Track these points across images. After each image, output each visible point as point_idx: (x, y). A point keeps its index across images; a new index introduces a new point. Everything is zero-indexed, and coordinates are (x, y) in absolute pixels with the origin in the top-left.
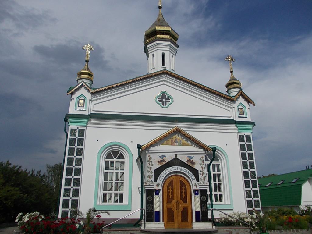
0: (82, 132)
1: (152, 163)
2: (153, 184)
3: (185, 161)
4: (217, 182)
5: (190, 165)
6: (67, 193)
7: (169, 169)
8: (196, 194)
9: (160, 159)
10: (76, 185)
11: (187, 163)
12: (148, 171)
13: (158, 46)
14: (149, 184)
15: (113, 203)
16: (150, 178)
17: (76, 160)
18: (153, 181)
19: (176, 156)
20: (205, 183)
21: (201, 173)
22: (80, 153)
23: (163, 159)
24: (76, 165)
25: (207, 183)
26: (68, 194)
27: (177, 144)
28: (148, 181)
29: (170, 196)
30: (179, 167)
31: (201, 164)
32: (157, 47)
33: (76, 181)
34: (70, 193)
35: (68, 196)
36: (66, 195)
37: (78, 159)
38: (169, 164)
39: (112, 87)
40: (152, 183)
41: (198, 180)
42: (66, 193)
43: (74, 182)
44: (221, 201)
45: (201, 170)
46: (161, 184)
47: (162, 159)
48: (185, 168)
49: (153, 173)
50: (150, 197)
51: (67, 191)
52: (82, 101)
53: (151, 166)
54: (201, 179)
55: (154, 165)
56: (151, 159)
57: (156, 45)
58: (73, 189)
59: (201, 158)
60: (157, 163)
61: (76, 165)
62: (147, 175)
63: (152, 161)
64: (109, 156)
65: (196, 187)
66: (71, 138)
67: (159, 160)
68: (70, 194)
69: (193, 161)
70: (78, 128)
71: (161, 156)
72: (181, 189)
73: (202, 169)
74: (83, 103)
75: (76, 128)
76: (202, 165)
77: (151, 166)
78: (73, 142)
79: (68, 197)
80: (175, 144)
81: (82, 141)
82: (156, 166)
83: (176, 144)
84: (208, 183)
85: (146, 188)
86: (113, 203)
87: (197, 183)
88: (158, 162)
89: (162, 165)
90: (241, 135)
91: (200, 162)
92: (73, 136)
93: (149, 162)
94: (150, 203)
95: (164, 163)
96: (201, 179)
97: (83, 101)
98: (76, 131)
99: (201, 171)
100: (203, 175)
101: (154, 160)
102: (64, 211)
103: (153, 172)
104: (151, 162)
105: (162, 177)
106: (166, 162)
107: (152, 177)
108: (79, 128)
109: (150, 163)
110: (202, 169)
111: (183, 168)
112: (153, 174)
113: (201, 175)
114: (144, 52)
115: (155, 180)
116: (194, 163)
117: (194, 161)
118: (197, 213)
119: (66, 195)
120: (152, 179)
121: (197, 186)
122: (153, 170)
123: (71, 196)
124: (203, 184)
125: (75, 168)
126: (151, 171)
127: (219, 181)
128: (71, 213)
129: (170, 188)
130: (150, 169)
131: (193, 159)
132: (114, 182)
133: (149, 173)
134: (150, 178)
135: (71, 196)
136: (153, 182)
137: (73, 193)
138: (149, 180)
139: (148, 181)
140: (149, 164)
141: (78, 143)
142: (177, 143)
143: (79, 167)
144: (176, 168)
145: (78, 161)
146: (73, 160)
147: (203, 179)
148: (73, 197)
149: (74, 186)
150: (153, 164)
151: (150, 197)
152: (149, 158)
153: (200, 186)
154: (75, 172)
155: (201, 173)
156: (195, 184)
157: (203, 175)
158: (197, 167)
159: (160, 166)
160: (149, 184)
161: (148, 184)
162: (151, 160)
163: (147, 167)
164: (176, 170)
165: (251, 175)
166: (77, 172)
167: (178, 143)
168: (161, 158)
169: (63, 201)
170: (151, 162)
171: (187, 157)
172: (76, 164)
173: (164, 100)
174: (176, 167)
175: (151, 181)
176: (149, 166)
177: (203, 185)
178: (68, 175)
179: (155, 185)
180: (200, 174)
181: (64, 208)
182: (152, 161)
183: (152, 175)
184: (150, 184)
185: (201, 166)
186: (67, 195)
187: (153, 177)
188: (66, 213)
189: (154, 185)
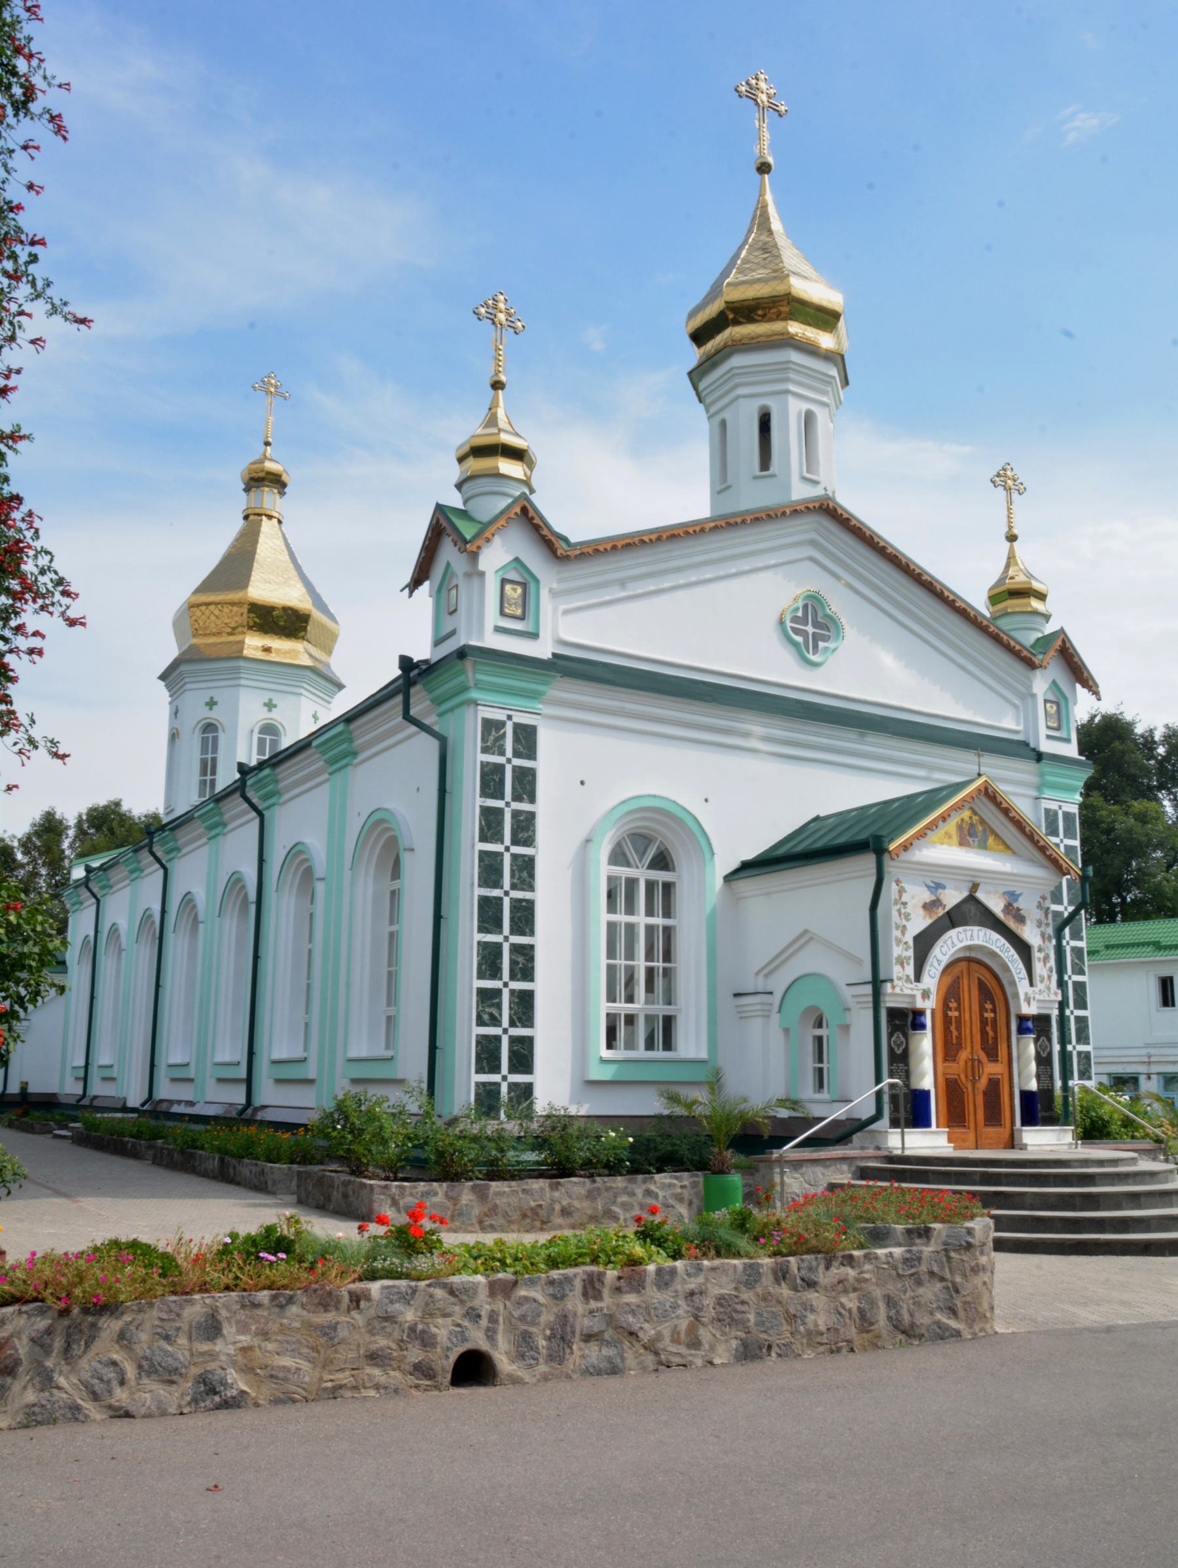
0: (526, 739)
1: (908, 910)
2: (912, 989)
3: (996, 906)
4: (659, 964)
5: (1011, 924)
6: (490, 1006)
7: (953, 933)
8: (1022, 1030)
9: (927, 897)
10: (519, 976)
11: (1001, 916)
12: (899, 942)
13: (792, 375)
14: (902, 990)
15: (641, 1053)
16: (903, 967)
17: (511, 865)
18: (912, 977)
20: (1052, 991)
21: (1041, 955)
22: (526, 835)
24: (514, 887)
25: (1056, 994)
26: (495, 1012)
27: (976, 843)
28: (899, 979)
29: (955, 1033)
31: (1039, 924)
32: (787, 380)
33: (521, 959)
34: (499, 1006)
35: (495, 1021)
36: (486, 1017)
37: (520, 861)
38: (954, 918)
39: (530, 515)
40: (910, 986)
41: (1031, 984)
42: (487, 1010)
43: (511, 960)
44: (668, 1045)
45: (1042, 943)
46: (933, 989)
47: (934, 898)
50: (898, 1037)
51: (488, 997)
52: (515, 590)
53: (904, 922)
54: (1040, 976)
55: (913, 916)
56: (904, 894)
57: (786, 366)
58: (512, 992)
59: (1041, 900)
60: (921, 912)
61: (514, 887)
62: (895, 955)
63: (906, 903)
64: (618, 857)
65: (1029, 1004)
66: (488, 763)
67: (928, 901)
68: (501, 1015)
69: (1018, 909)
70: (510, 717)
71: (933, 885)
72: (982, 1009)
74: (520, 601)
75: (504, 718)
76: (1042, 929)
77: (904, 922)
78: (494, 780)
79: (495, 1026)
80: (970, 840)
81: (531, 778)
82: (919, 922)
84: (1059, 992)
86: (641, 1053)
87: (1030, 990)
88: (926, 907)
89: (935, 918)
90: (1050, 810)
91: (1038, 917)
92: (493, 754)
93: (898, 907)
94: (901, 1060)
95: (941, 912)
96: (1040, 976)
97: (519, 590)
98: (505, 733)
99: (1040, 950)
100: (1045, 965)
101: (913, 897)
102: (484, 1084)
103: (911, 943)
104: (905, 904)
105: (935, 964)
106: (947, 909)
107: (908, 964)
108: (515, 720)
109: (903, 911)
111: (995, 936)
112: (910, 953)
113: (1042, 963)
114: (690, 374)
115: (918, 977)
116: (1021, 919)
117: (1021, 912)
118: (1027, 1096)
119: (486, 1017)
120: (910, 970)
121: (1032, 1000)
122: (909, 938)
123: (505, 1022)
124: (1046, 994)
125: (501, 899)
126: (904, 940)
127: (667, 957)
128: (512, 1094)
129: (953, 1005)
130: (903, 933)
131: (1021, 904)
133: (901, 947)
134: (903, 967)
135: (505, 1022)
137: (511, 1008)
138: (900, 975)
139: (899, 979)
140: (900, 915)
141: (513, 788)
143: (527, 895)
144: (975, 934)
145: (521, 871)
146: (502, 860)
147: (1046, 977)
148: (512, 1024)
149: (513, 977)
150: (909, 914)
151: (898, 1037)
152: (899, 891)
153: (1039, 1001)
154: (512, 919)
155: (1041, 955)
156: (1026, 994)
157: (1045, 965)
158: (1030, 934)
159: (928, 922)
160: (902, 990)
161: (897, 990)
163: (893, 925)
164: (976, 942)
165: (1072, 961)
166: (520, 918)
167: (977, 837)
168: (932, 893)
169: (478, 1043)
170: (905, 904)
171: (1004, 893)
172: (515, 881)
173: (810, 629)
174: (976, 928)
175: (908, 976)
177: (1047, 998)
178: (488, 931)
180: (1039, 959)
181: (484, 1073)
182: (906, 903)
183: (910, 957)
186: (492, 1016)
187: (912, 962)
188: (491, 1091)
189: (915, 992)
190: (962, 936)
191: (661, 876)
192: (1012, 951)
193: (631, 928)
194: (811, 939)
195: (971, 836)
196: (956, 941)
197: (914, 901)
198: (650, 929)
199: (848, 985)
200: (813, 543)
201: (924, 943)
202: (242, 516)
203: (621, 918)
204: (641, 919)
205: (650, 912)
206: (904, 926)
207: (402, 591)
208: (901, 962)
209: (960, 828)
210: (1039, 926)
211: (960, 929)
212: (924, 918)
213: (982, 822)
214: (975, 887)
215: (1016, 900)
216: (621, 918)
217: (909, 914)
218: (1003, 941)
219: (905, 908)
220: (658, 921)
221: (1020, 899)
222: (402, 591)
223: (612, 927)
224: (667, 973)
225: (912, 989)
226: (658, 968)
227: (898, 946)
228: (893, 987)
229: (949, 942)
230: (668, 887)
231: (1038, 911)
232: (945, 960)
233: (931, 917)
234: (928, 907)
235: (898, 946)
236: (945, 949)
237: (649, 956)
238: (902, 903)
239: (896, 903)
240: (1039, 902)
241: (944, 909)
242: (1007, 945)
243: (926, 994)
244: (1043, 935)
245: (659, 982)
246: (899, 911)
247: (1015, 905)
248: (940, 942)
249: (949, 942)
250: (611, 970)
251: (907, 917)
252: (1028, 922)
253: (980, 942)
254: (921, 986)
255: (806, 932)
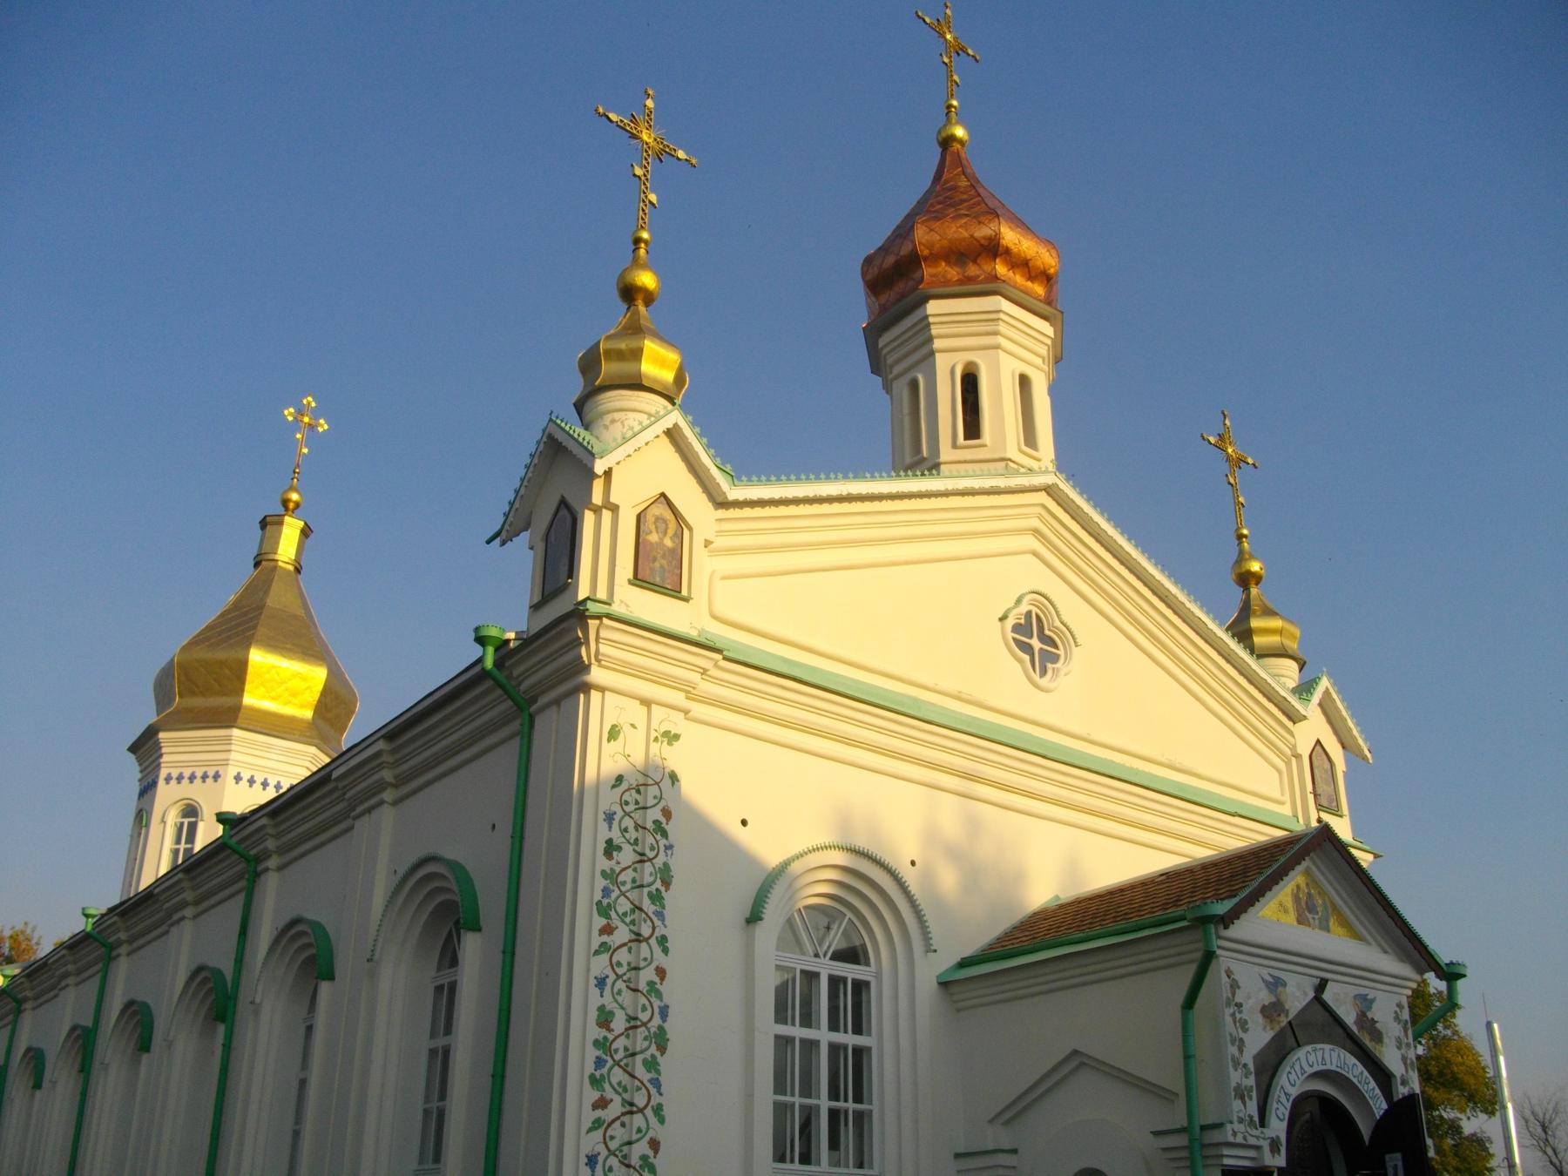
2: (1258, 1138)
5: (1367, 1041)
9: (1265, 997)
11: (1355, 1029)
14: (1245, 1138)
16: (1244, 1103)
18: (1256, 1119)
19: (1321, 986)
23: (1276, 996)
30: (1338, 1049)
40: (1254, 1132)
45: (1404, 1073)
48: (1354, 1061)
49: (1251, 1073)
55: (1250, 1025)
59: (1398, 1009)
60: (1260, 1019)
69: (1373, 1021)
71: (1270, 979)
73: (1407, 1071)
80: (1310, 916)
82: (1258, 1037)
83: (1311, 921)
85: (1227, 1161)
89: (1277, 1028)
91: (1397, 1034)
93: (1232, 1011)
95: (1284, 1021)
101: (1249, 997)
103: (1251, 1067)
104: (1239, 1005)
105: (1283, 1099)
107: (1251, 1098)
109: (1238, 1016)
110: (1407, 1071)
111: (1352, 1060)
115: (1263, 1122)
116: (1377, 1036)
117: (1377, 1025)
122: (1248, 1058)
130: (1241, 1051)
132: (824, 1103)
134: (1244, 1103)
136: (1257, 1129)
138: (1241, 1115)
139: (1241, 1121)
140: (1235, 1022)
142: (1316, 917)
152: (1231, 986)
160: (1245, 1138)
161: (1239, 1139)
162: (1238, 999)
163: (1228, 1038)
164: (1328, 1067)
167: (1317, 913)
168: (1271, 991)
170: (1239, 1005)
171: (1356, 997)
174: (1327, 1047)
175: (1251, 1117)
176: (1235, 1033)
179: (1265, 1144)
184: (1249, 1138)
185: (1402, 1051)
187: (1254, 1094)
189: (1261, 1142)
190: (1312, 1058)
191: (850, 971)
192: (1373, 1084)
193: (810, 1046)
194: (1082, 1064)
195: (1310, 913)
196: (1307, 1068)
197: (1251, 1002)
198: (835, 1049)
199: (1156, 1134)
200: (1036, 532)
201: (1270, 1065)
202: (253, 563)
203: (798, 1032)
204: (823, 1035)
205: (834, 1026)
206: (1241, 1040)
207: (488, 542)
208: (1241, 1094)
209: (1296, 899)
210: (1399, 1048)
211: (1309, 1048)
212: (1264, 1028)
213: (1322, 893)
214: (1321, 986)
215: (1370, 1008)
216: (798, 1032)
217: (1246, 1022)
218: (1361, 1067)
219: (1240, 1012)
220: (849, 1039)
221: (1375, 1006)
222: (488, 542)
223: (783, 1043)
224: (860, 1118)
225: (1258, 1138)
226: (846, 1112)
227: (1236, 1070)
228: (1235, 1134)
229: (1297, 1067)
230: (860, 987)
231: (1395, 1024)
232: (1294, 1092)
233: (1272, 1029)
234: (1271, 1011)
235: (1236, 1070)
236: (1293, 1076)
237: (834, 1094)
238: (1236, 1005)
239: (1228, 1004)
240: (1396, 1012)
241: (1287, 1016)
242: (1366, 1073)
243: (1274, 1146)
244: (1404, 1059)
245: (848, 1136)
246: (1233, 1015)
247: (1370, 1015)
248: (1286, 1068)
249: (1297, 1067)
250: (781, 1110)
251: (1244, 1025)
252: (1386, 1040)
253: (1333, 1068)
254: (1269, 1133)
255: (1075, 1053)
